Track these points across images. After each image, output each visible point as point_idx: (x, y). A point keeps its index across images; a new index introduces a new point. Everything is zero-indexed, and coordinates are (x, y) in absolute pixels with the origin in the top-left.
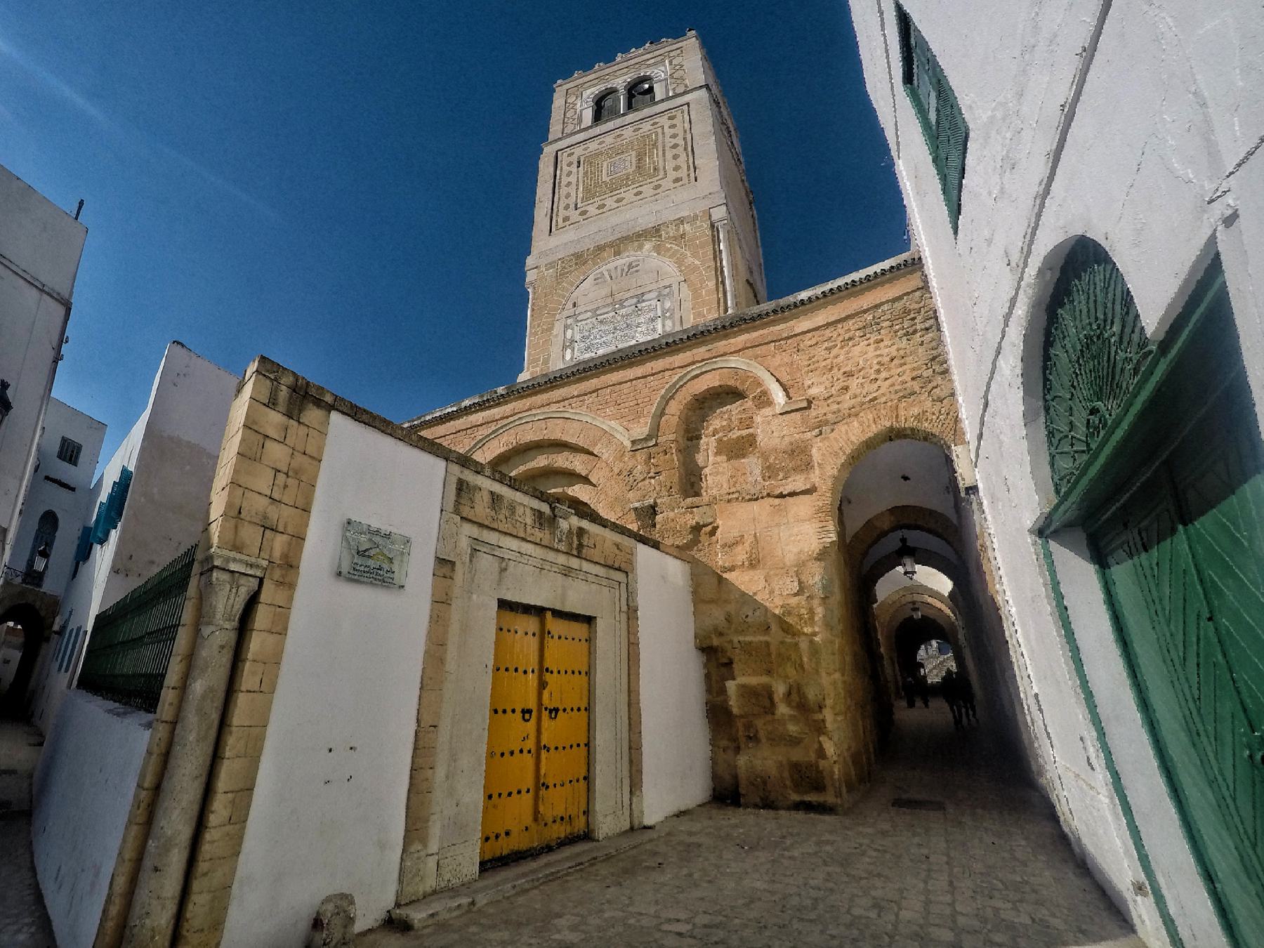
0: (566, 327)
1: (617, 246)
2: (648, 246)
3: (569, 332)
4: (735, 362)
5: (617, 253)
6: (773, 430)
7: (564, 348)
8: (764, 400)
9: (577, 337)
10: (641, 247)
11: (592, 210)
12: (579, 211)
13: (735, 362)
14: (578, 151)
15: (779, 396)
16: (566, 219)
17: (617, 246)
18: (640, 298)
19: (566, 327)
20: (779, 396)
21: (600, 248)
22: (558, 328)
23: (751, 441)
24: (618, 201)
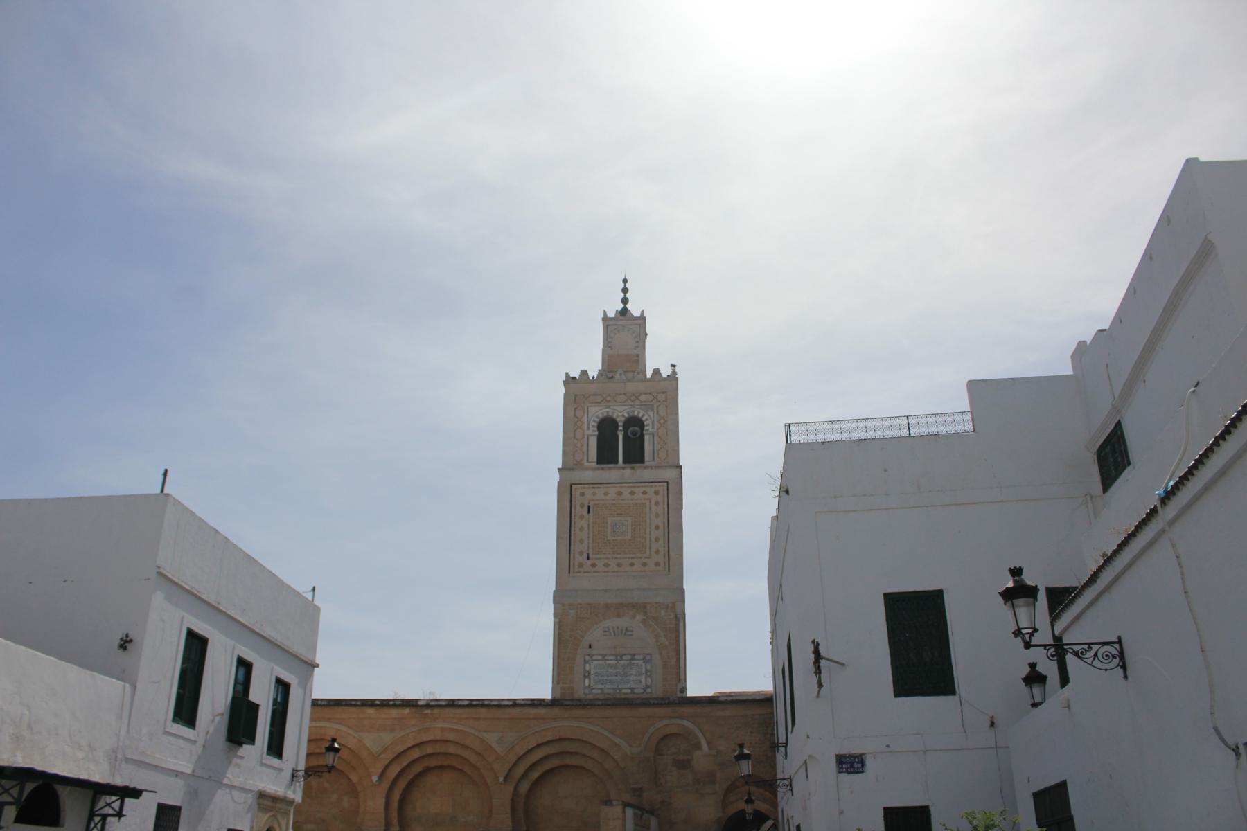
0: (586, 662)
1: (619, 609)
2: (639, 617)
3: (587, 667)
4: (686, 723)
5: (619, 616)
6: (702, 760)
7: (585, 677)
8: (698, 746)
9: (593, 671)
10: (634, 617)
11: (600, 564)
12: (590, 562)
13: (686, 723)
14: (589, 492)
15: (705, 746)
16: (581, 565)
17: (619, 609)
18: (633, 657)
19: (586, 662)
20: (705, 746)
21: (607, 606)
22: (579, 659)
23: (689, 762)
24: (619, 565)
